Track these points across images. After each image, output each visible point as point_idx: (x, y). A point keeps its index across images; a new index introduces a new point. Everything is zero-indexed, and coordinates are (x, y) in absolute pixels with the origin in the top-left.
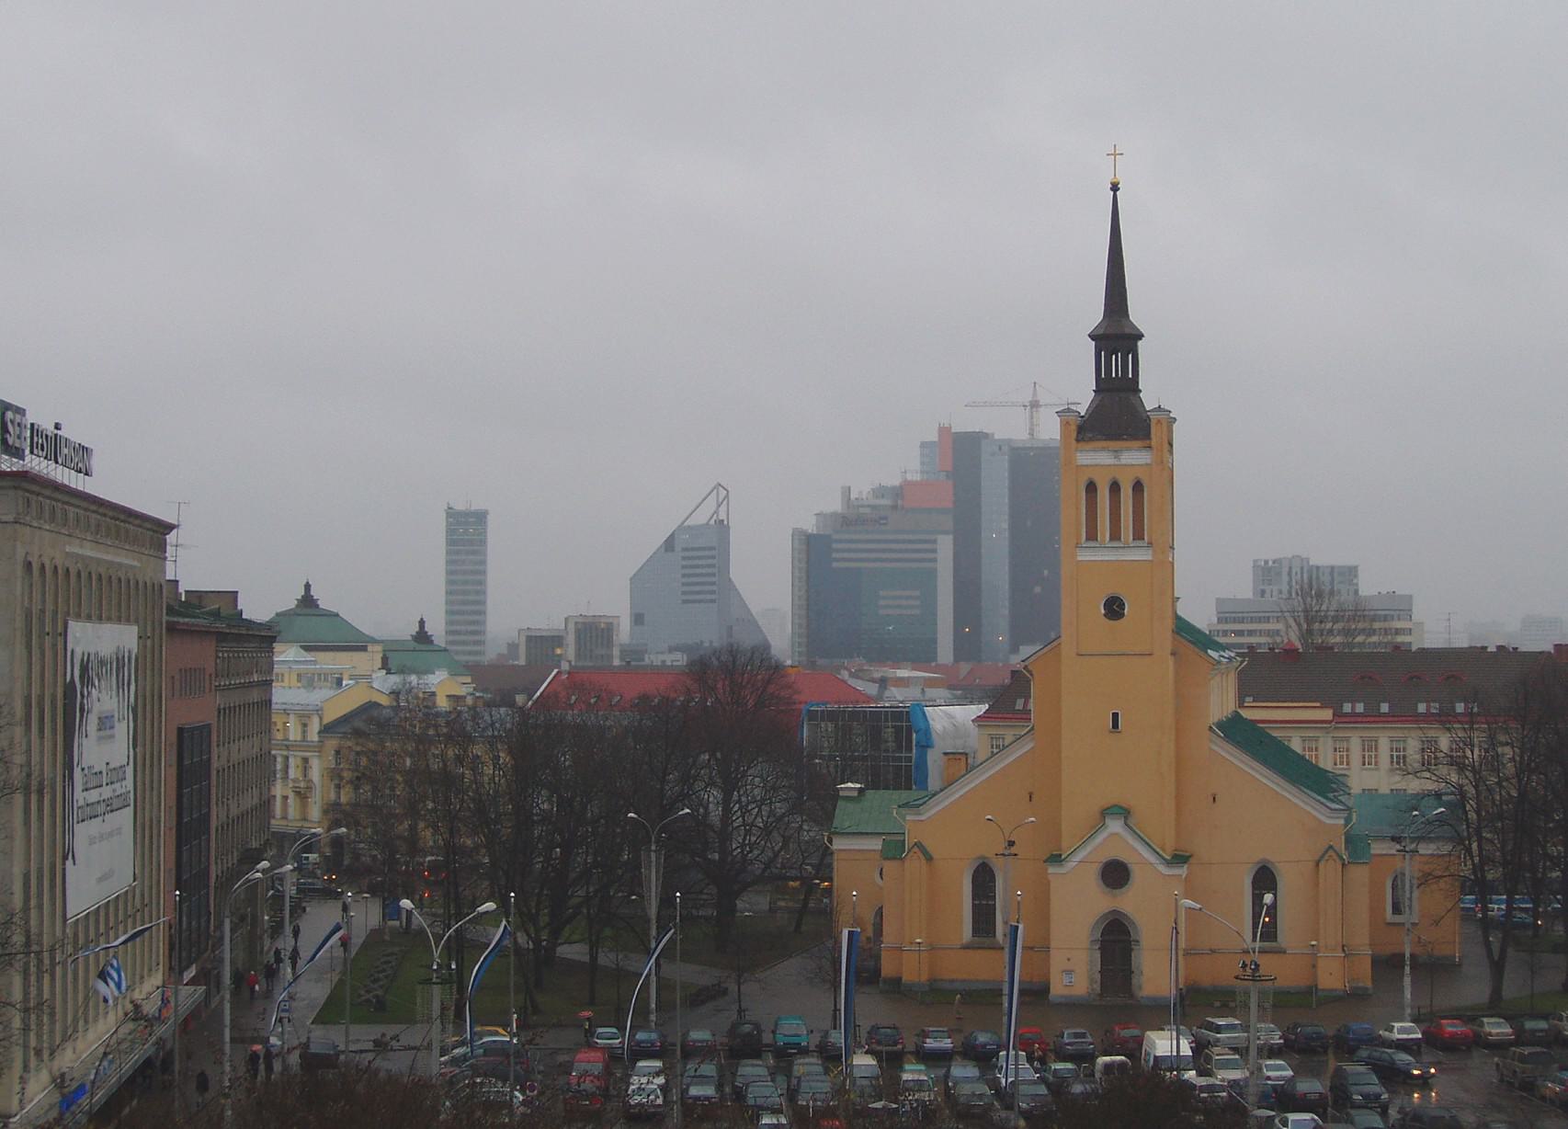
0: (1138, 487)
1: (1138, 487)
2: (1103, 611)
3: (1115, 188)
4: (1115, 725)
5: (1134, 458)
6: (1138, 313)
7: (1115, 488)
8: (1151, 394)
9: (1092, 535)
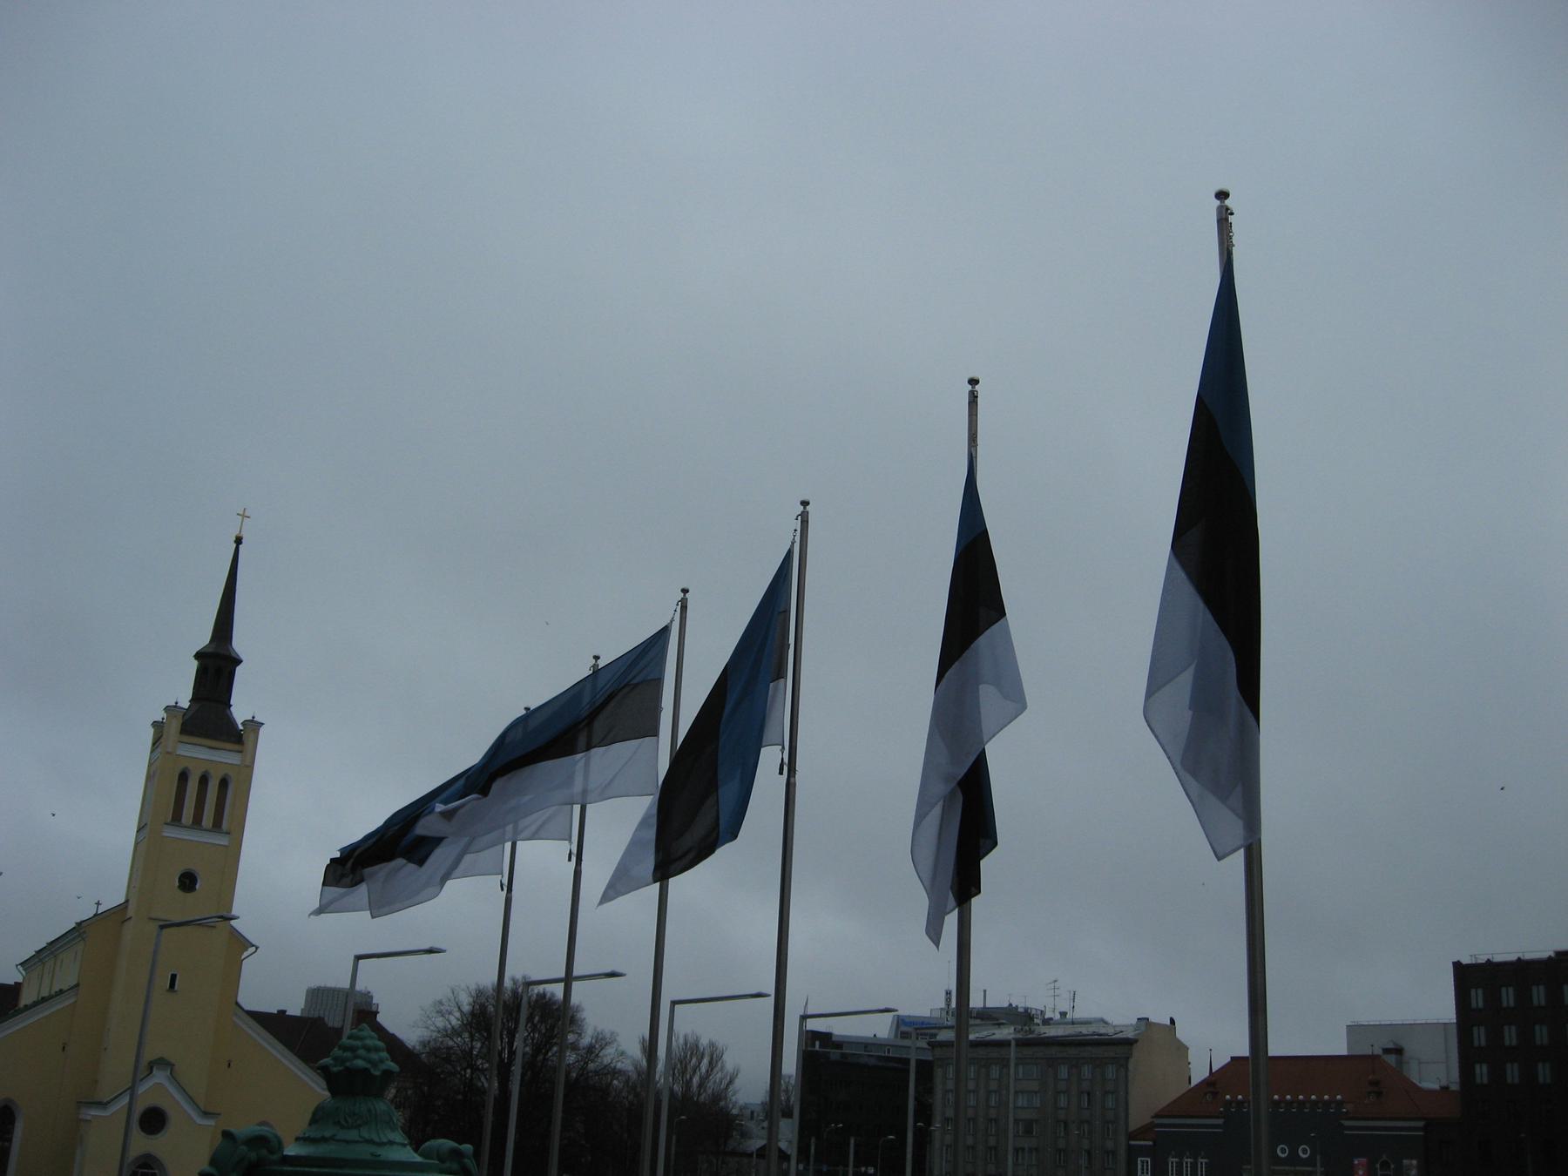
0: (224, 783)
1: (224, 783)
3: (239, 541)
5: (218, 757)
6: (241, 643)
7: (204, 780)
8: (241, 710)
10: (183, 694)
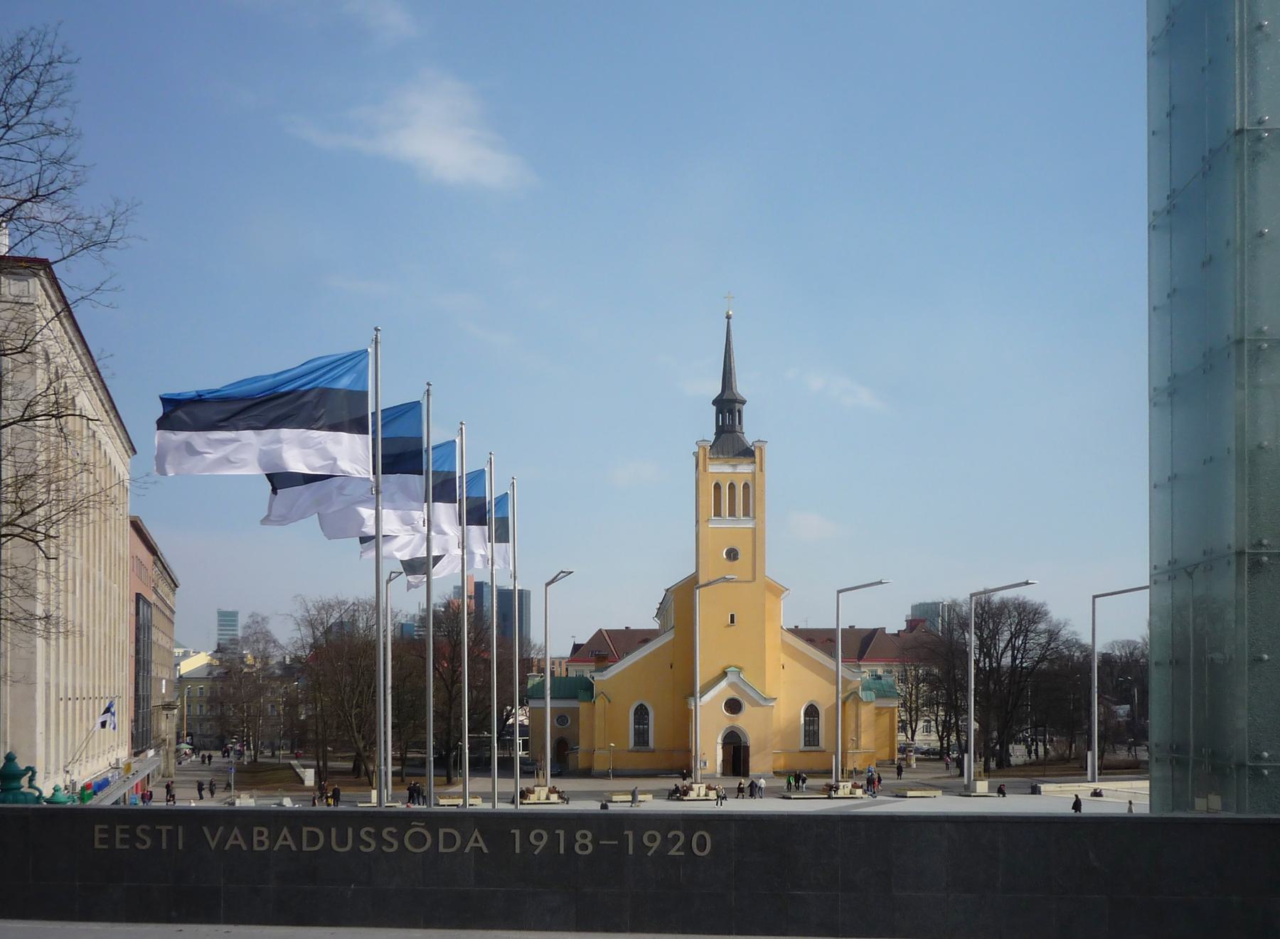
1: (746, 486)
2: (725, 557)
3: (728, 317)
4: (732, 621)
6: (742, 388)
7: (732, 486)
9: (718, 513)
10: (709, 433)
